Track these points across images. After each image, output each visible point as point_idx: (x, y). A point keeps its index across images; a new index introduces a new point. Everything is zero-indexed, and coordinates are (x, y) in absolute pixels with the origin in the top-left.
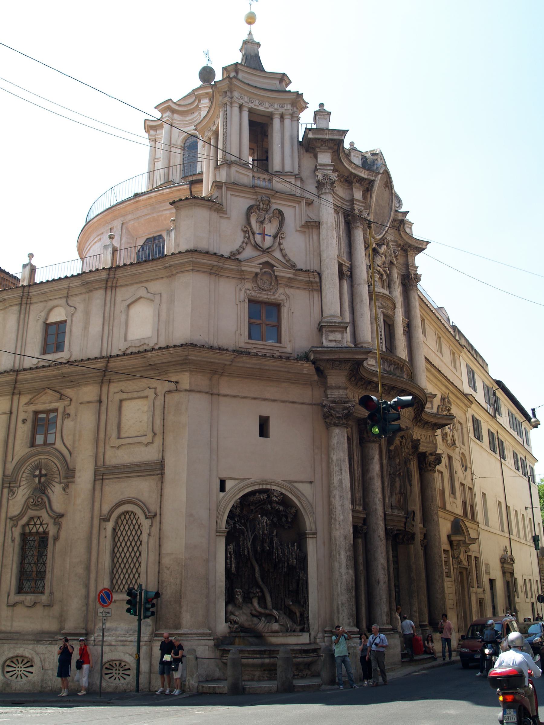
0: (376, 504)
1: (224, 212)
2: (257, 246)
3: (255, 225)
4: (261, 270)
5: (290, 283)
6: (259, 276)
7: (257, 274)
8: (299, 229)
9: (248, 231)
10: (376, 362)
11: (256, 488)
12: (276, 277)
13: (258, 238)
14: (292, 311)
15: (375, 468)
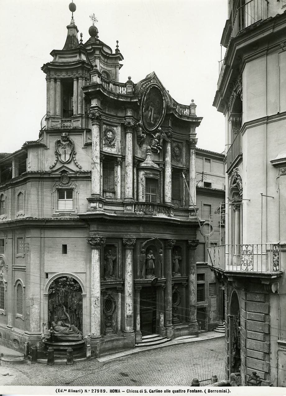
0: (127, 278)
1: (46, 146)
2: (62, 162)
3: (61, 151)
4: (61, 174)
5: (76, 178)
6: (61, 178)
7: (60, 177)
8: (83, 147)
9: (57, 154)
10: (132, 208)
11: (59, 277)
12: (70, 178)
13: (62, 158)
14: (78, 193)
15: (129, 260)
